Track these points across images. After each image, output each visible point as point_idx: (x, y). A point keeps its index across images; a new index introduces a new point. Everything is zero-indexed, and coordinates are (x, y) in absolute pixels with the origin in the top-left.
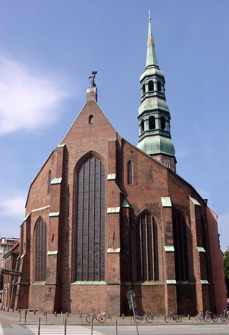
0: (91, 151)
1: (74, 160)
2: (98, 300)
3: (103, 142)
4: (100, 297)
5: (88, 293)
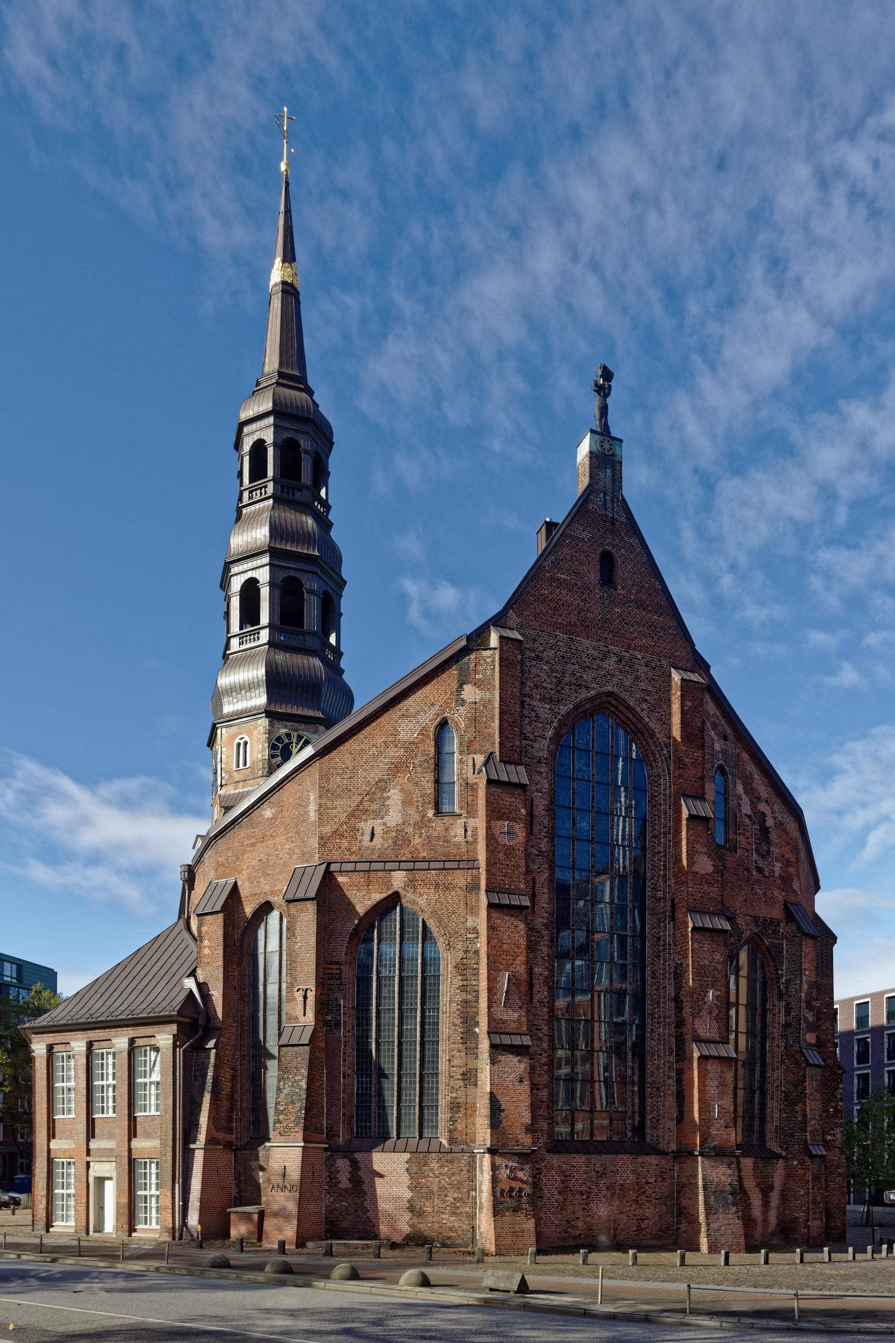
0: (609, 694)
1: (548, 706)
2: (637, 1201)
4: (644, 1192)
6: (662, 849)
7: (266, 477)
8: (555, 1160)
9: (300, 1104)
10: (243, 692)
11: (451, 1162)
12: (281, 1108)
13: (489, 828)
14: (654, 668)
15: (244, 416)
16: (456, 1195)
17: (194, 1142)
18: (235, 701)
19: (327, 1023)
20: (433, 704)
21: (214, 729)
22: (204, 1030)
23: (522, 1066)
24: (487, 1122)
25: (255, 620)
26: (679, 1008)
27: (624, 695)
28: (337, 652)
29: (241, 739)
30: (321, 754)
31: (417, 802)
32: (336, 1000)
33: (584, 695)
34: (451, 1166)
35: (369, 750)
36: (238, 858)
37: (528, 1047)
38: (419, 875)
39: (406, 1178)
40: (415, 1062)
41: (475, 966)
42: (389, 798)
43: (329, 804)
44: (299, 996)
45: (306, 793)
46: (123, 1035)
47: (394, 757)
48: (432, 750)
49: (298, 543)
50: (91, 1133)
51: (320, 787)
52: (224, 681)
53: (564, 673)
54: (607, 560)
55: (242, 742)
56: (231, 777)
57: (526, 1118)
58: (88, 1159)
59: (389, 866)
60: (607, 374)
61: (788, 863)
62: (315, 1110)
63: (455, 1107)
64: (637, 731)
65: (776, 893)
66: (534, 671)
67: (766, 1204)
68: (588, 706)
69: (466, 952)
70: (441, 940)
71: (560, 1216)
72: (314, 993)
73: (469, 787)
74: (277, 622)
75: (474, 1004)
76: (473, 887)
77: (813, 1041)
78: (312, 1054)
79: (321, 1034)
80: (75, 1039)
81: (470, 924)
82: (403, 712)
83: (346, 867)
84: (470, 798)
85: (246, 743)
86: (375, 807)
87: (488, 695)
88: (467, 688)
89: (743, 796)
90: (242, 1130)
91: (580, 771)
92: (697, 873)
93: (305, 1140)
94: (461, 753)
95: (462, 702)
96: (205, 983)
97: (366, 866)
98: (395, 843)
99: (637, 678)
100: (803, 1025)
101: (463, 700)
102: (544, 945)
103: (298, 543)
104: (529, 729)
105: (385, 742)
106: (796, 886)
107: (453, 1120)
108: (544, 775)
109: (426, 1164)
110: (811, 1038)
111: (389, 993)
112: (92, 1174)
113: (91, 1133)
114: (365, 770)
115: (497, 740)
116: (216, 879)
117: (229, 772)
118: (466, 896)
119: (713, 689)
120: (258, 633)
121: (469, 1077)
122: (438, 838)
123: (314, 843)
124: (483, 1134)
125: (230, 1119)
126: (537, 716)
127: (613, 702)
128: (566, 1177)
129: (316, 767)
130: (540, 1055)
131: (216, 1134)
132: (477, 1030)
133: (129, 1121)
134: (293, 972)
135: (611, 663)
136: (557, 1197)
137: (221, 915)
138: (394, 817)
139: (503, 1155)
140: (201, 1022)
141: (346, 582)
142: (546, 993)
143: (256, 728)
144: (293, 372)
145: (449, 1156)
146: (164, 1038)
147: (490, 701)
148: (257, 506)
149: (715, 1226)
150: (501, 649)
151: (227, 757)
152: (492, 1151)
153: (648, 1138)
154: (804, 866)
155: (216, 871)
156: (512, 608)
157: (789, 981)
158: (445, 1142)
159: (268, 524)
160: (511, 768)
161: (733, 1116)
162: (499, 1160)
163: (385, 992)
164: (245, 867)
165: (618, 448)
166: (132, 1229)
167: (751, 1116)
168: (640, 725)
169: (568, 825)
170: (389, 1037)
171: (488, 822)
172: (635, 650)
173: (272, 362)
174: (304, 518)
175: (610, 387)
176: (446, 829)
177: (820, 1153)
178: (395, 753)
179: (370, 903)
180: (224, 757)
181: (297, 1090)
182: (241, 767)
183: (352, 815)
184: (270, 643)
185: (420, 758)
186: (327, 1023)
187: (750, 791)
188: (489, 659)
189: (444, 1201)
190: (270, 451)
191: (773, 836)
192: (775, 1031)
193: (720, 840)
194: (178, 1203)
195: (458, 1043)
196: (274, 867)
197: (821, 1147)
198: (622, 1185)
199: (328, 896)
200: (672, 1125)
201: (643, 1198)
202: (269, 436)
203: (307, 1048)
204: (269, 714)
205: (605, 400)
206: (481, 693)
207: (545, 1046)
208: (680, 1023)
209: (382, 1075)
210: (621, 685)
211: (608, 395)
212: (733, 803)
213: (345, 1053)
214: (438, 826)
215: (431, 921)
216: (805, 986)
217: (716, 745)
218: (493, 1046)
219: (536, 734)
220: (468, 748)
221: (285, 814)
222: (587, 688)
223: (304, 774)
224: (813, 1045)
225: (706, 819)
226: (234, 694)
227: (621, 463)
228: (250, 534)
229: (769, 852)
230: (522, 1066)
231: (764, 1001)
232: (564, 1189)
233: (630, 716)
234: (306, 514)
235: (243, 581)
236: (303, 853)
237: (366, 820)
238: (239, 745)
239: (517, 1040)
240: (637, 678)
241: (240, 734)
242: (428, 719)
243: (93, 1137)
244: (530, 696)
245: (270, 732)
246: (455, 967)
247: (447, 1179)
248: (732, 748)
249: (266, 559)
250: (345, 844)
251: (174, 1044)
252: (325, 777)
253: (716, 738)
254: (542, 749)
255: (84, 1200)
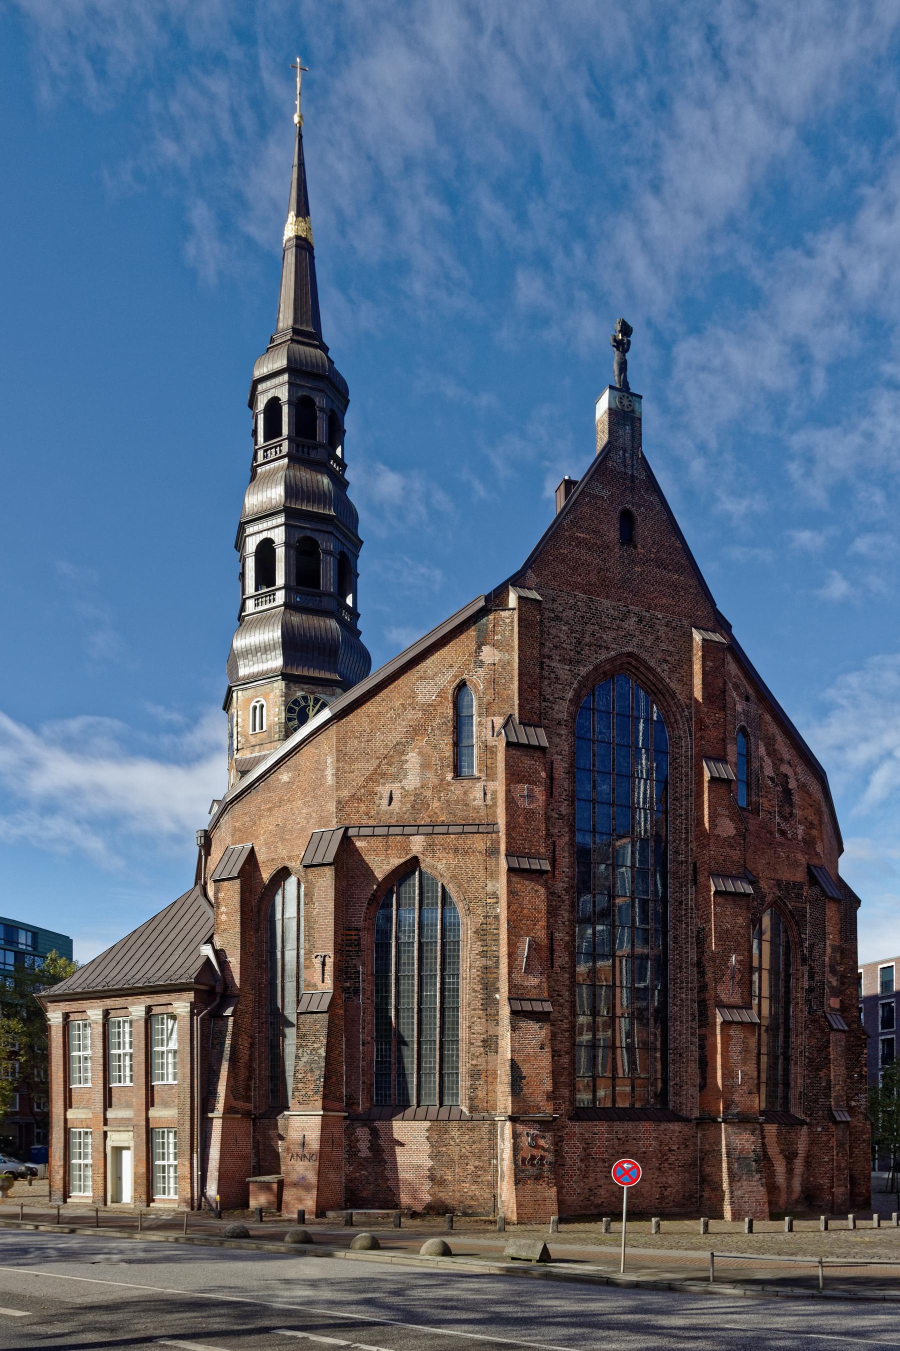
0: (630, 655)
1: (567, 667)
2: (660, 1169)
3: (671, 635)
4: (667, 1160)
5: (628, 1148)
6: (683, 812)
7: (281, 435)
8: (577, 1128)
9: (319, 1072)
10: (259, 654)
11: (472, 1129)
12: (300, 1076)
13: (508, 792)
14: (674, 629)
15: (258, 373)
16: (477, 1163)
17: (212, 1111)
18: (251, 663)
19: (346, 990)
20: (451, 666)
21: (230, 692)
22: (221, 998)
23: (544, 1032)
24: (508, 1089)
25: (271, 581)
26: (702, 973)
27: (645, 656)
28: (354, 613)
29: (257, 702)
30: (338, 717)
31: (436, 765)
32: (355, 966)
33: (603, 656)
34: (471, 1134)
35: (387, 712)
36: (255, 823)
37: (549, 1013)
38: (438, 839)
39: (426, 1146)
40: (435, 1029)
41: (495, 931)
42: (407, 761)
43: (347, 767)
44: (317, 963)
45: (323, 757)
46: (140, 1003)
47: (412, 720)
48: (450, 712)
49: (314, 503)
50: (108, 1102)
51: (338, 751)
52: (240, 643)
53: (583, 633)
54: (627, 520)
55: (258, 705)
56: (247, 740)
57: (548, 1085)
58: (106, 1129)
59: (407, 830)
60: (626, 329)
61: (811, 826)
62: (334, 1078)
63: (475, 1074)
64: (658, 692)
65: (799, 856)
66: (553, 631)
67: (790, 1171)
68: (608, 667)
69: (486, 917)
70: (461, 905)
71: (582, 1184)
72: (332, 959)
73: (489, 750)
74: (293, 583)
75: (495, 970)
76: (493, 852)
77: (837, 1006)
78: (331, 1021)
79: (339, 1001)
80: (91, 1008)
81: (490, 888)
82: (421, 674)
83: (364, 831)
84: (489, 761)
85: (262, 706)
86: (393, 770)
87: (507, 657)
88: (486, 649)
89: (766, 758)
90: (262, 1100)
91: (600, 733)
92: (719, 836)
93: (324, 1109)
94: (480, 715)
95: (481, 664)
96: (222, 950)
97: (384, 831)
98: (413, 807)
99: (658, 638)
100: (827, 990)
101: (481, 661)
102: (565, 910)
103: (314, 503)
104: (549, 690)
105: (403, 705)
106: (819, 848)
107: (474, 1088)
108: (564, 737)
109: (446, 1132)
110: (835, 1003)
111: (408, 959)
112: (109, 1144)
113: (108, 1102)
114: (383, 733)
115: (517, 702)
116: (233, 844)
117: (246, 736)
118: (485, 861)
119: (735, 650)
120: (274, 595)
121: (490, 1044)
122: (457, 802)
123: (332, 807)
124: (504, 1102)
125: (248, 1088)
126: (557, 678)
127: (634, 663)
128: (588, 1145)
129: (333, 729)
130: (562, 1021)
131: (234, 1103)
132: (497, 996)
133: (147, 1089)
134: (311, 938)
135: (631, 624)
136: (579, 1164)
137: (238, 881)
138: (412, 781)
139: (524, 1123)
140: (219, 989)
141: (362, 542)
142: (567, 959)
143: (272, 690)
144: (307, 330)
145: (470, 1124)
146: (182, 1005)
147: (509, 663)
148: (272, 465)
149: (738, 1193)
150: (520, 609)
151: (243, 720)
152: (513, 1119)
153: (671, 1105)
154: (828, 828)
155: (233, 836)
156: (531, 568)
157: (812, 945)
158: (465, 1110)
159: (283, 484)
160: (530, 730)
161: (756, 1082)
162: (520, 1128)
163: (404, 958)
164: (262, 832)
165: (637, 405)
166: (150, 1200)
167: (777, 1082)
168: (661, 686)
169: (589, 787)
170: (408, 1004)
171: (507, 785)
172: (655, 609)
173: (286, 319)
174: (319, 477)
175: (629, 342)
176: (465, 793)
177: (844, 1119)
178: (414, 716)
179: (388, 868)
180: (240, 720)
181: (316, 1058)
182: (257, 731)
183: (370, 779)
184: (286, 605)
185: (438, 721)
186: (346, 990)
187: (772, 752)
188: (507, 621)
189: (465, 1170)
190: (285, 409)
191: (796, 798)
192: (799, 996)
193: (743, 803)
194: (197, 1173)
195: (479, 1010)
196: (291, 832)
197: (846, 1114)
198: (645, 1153)
199: (347, 861)
200: (694, 1091)
201: (666, 1165)
202: (283, 394)
203: (326, 1016)
204: (285, 676)
205: (624, 355)
206: (498, 655)
207: (566, 1012)
208: (703, 988)
209: (402, 1042)
210: (641, 646)
211: (627, 350)
212: (755, 765)
213: (364, 1021)
214: (457, 789)
215: (450, 885)
216: (829, 950)
217: (738, 705)
218: (514, 1013)
219: (556, 696)
220: (487, 710)
221: (302, 778)
222: (607, 648)
223: (321, 737)
224: (837, 1010)
225: (728, 782)
226: (250, 656)
227: (640, 419)
228: (265, 494)
229: (791, 814)
230: (544, 1032)
231: (788, 965)
232: (587, 1157)
233: (651, 677)
234: (322, 473)
235: (258, 542)
236: (321, 818)
237: (384, 784)
238: (255, 708)
239: (538, 1007)
240: (658, 638)
241: (256, 697)
242: (447, 681)
243: (110, 1106)
244: (550, 657)
245: (286, 695)
246: (475, 932)
247: (468, 1147)
248: (754, 708)
249: (281, 519)
250: (363, 808)
251: (192, 1011)
252: (342, 740)
253: (737, 699)
254: (562, 710)
255: (102, 1170)
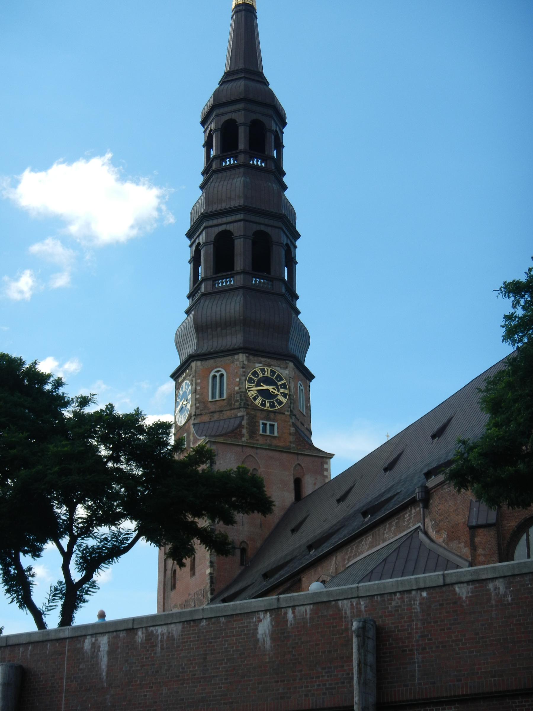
10: (219, 329)
29: (218, 372)
55: (218, 375)
85: (222, 376)
143: (233, 362)
226: (209, 330)
238: (214, 377)
